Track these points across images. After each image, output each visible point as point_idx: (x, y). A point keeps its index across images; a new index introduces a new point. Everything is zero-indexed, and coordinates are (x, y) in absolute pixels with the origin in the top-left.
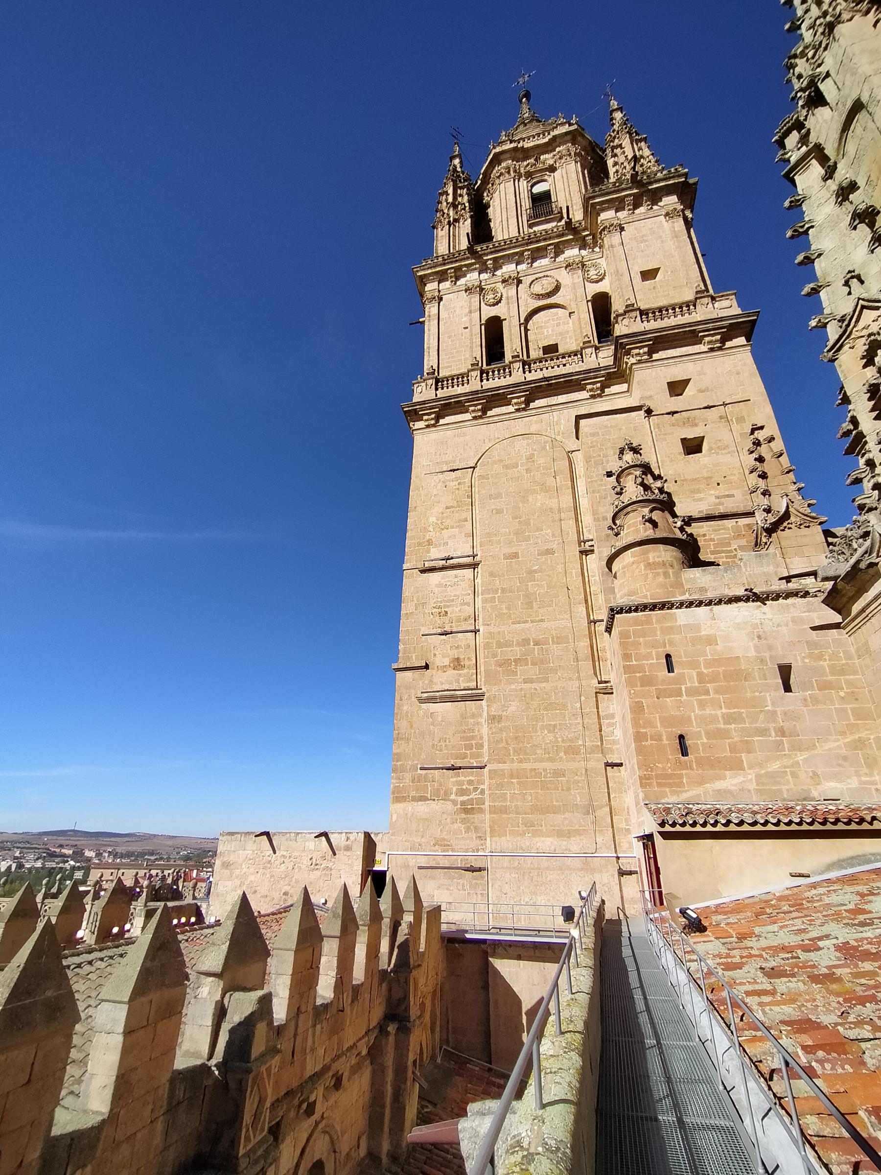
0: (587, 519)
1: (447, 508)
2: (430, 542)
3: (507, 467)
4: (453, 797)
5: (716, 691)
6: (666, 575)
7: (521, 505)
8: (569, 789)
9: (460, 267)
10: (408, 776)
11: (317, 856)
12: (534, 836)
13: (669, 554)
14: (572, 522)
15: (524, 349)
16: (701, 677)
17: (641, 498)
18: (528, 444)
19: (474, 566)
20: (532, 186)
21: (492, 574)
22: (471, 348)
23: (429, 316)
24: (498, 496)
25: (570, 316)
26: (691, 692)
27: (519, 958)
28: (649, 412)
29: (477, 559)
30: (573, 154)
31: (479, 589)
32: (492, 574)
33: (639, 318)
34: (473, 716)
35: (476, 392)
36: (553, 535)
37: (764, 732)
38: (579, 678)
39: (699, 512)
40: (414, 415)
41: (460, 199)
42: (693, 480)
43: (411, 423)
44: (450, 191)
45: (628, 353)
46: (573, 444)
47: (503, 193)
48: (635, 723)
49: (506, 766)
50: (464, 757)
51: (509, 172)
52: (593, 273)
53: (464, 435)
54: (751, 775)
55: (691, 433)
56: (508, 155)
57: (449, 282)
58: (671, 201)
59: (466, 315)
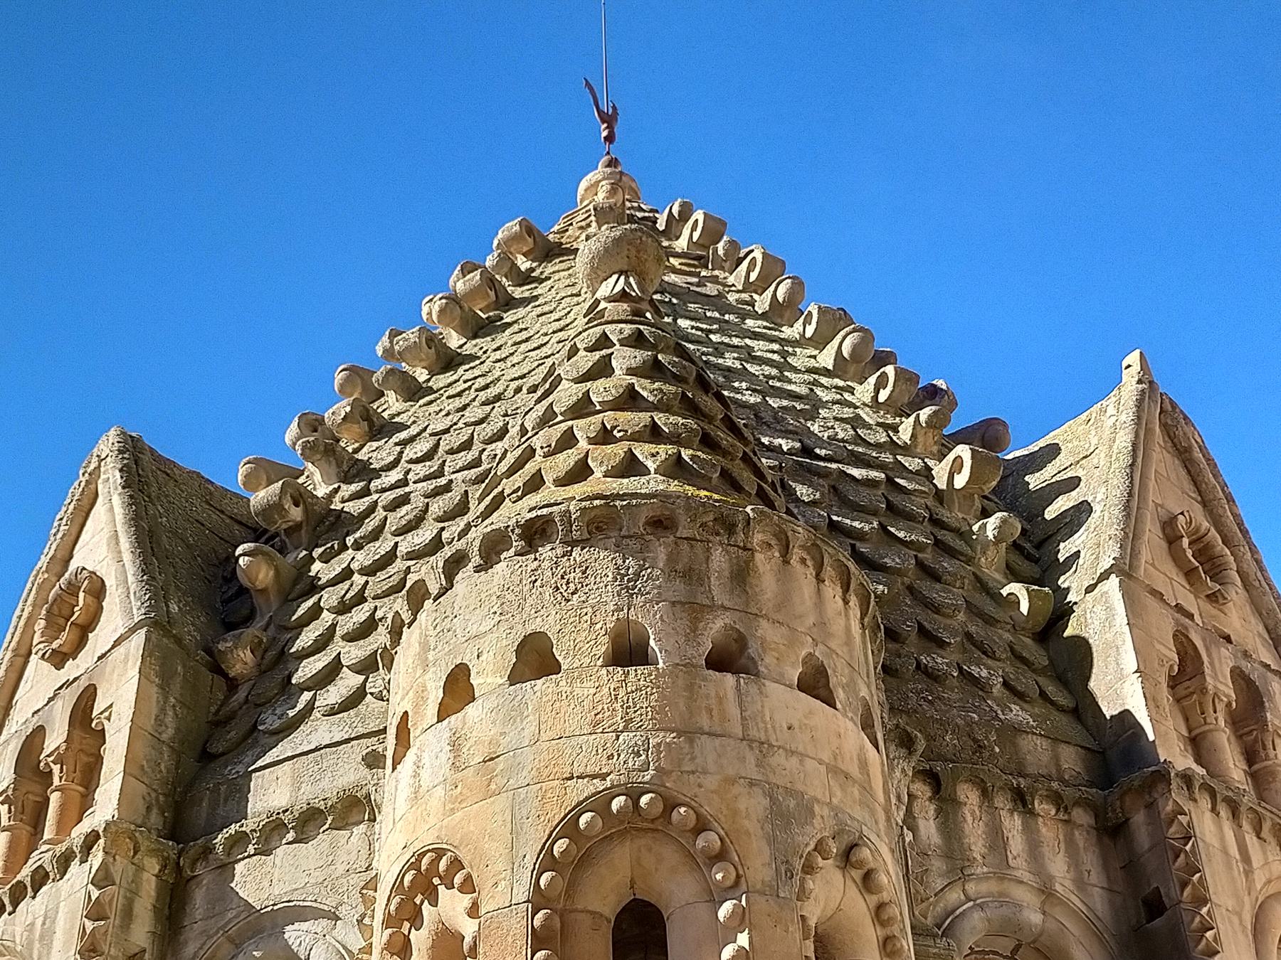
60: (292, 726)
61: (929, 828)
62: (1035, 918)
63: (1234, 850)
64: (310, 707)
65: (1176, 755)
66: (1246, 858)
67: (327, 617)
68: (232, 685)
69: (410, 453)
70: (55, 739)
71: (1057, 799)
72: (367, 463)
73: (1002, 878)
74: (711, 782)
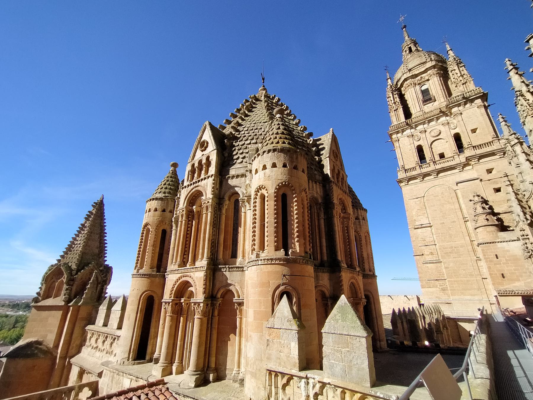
0: (465, 211)
1: (418, 210)
2: (415, 220)
3: (435, 196)
4: (438, 287)
5: (511, 263)
6: (493, 234)
7: (442, 208)
8: (472, 285)
9: (403, 129)
10: (424, 282)
11: (405, 301)
12: (464, 296)
13: (493, 228)
14: (460, 212)
15: (433, 156)
16: (506, 260)
17: (482, 213)
18: (441, 189)
19: (431, 227)
20: (421, 88)
21: (437, 229)
22: (414, 157)
23: (396, 147)
24: (434, 205)
25: (457, 185)
26: (503, 263)
27: (465, 322)
28: (481, 180)
29: (431, 224)
30: (435, 74)
31: (434, 233)
32: (437, 229)
33: (473, 149)
34: (440, 267)
35: (420, 174)
36: (455, 217)
37: (526, 273)
38: (470, 257)
39: (502, 211)
40: (400, 181)
41: (396, 99)
42: (499, 201)
43: (399, 184)
44: (391, 95)
45: (471, 161)
46: (455, 187)
47: (410, 93)
48: (489, 271)
49: (453, 279)
50: (440, 277)
51: (411, 85)
52: (452, 126)
53: (418, 186)
54: (523, 282)
55: (497, 186)
56: (410, 78)
57: (400, 134)
58: (479, 101)
59: (409, 145)
60: (234, 164)
62: (316, 195)
64: (236, 162)
65: (332, 179)
68: (225, 157)
69: (245, 129)
71: (319, 183)
72: (239, 130)
73: (313, 191)
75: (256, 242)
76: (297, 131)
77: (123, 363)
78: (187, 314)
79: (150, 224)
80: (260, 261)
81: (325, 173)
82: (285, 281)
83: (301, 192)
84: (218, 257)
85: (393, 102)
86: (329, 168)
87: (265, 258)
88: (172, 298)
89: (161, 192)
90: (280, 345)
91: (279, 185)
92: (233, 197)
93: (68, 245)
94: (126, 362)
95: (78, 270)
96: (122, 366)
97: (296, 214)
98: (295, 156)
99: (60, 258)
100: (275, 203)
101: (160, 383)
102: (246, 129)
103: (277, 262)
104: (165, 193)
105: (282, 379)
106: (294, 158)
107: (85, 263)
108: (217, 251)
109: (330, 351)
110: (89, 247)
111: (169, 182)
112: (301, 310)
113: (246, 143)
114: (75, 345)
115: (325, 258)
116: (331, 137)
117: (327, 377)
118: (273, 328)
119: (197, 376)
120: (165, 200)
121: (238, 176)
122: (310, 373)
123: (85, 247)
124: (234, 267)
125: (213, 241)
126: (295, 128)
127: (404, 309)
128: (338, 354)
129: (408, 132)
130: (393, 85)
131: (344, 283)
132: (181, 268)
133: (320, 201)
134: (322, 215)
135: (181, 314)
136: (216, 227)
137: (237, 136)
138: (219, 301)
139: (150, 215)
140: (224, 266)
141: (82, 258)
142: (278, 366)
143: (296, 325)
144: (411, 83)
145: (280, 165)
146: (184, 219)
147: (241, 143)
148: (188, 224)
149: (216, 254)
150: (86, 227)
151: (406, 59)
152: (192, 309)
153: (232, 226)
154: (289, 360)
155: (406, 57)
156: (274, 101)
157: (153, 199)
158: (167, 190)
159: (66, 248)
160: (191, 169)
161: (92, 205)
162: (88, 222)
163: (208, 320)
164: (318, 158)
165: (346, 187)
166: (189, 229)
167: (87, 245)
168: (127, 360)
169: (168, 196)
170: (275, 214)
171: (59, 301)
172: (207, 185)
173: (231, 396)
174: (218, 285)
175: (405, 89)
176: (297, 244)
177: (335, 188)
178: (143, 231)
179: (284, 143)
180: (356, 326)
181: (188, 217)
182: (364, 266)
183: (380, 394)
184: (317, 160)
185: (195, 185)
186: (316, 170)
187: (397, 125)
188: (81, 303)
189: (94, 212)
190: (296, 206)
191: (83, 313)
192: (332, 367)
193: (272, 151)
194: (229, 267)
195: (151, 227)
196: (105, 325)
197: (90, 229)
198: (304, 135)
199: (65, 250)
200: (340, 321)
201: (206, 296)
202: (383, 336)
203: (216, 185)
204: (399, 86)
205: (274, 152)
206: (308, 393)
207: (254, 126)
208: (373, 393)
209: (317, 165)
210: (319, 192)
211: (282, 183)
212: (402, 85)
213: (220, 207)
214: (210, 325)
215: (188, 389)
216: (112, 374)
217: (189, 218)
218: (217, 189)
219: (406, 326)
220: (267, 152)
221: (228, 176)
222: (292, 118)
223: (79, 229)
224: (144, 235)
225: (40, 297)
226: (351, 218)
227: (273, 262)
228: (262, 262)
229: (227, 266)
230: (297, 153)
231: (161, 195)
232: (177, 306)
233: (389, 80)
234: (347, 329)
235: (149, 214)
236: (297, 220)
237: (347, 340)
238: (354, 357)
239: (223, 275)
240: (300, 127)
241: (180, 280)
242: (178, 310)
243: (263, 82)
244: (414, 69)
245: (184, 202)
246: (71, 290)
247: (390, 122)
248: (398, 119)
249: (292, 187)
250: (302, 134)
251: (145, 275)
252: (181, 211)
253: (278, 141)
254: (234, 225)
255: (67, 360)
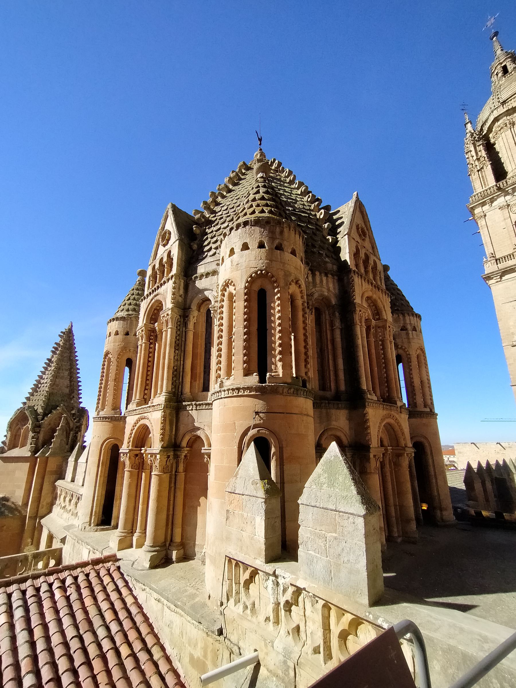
9: (493, 198)
23: (481, 226)
40: (488, 278)
41: (479, 154)
44: (472, 149)
51: (506, 126)
57: (488, 205)
61: (310, 279)
62: (326, 294)
63: (360, 284)
66: (362, 285)
67: (209, 239)
68: (194, 251)
70: (165, 260)
74: (275, 269)
75: (221, 366)
76: (302, 203)
77: (85, 529)
78: (151, 469)
79: (110, 353)
80: (223, 393)
81: (342, 260)
82: (258, 422)
83: (288, 284)
84: (183, 391)
85: (475, 158)
86: (347, 251)
87: (229, 387)
88: (130, 448)
89: (123, 310)
90: (242, 519)
91: (252, 275)
92: (203, 305)
93: (34, 385)
94: (88, 528)
95: (45, 415)
96: (83, 532)
97: (279, 318)
98: (278, 230)
99: (25, 401)
100: (246, 303)
101: (109, 559)
102: (225, 208)
103: (246, 393)
104: (128, 310)
105: (244, 571)
106: (277, 233)
107: (53, 405)
108: (182, 382)
109: (309, 535)
110: (57, 386)
111: (134, 296)
112: (283, 465)
113: (222, 227)
114: (45, 503)
115: (343, 387)
116: (353, 205)
117: (303, 578)
118: (234, 493)
119: (154, 553)
120: (128, 320)
121: (207, 275)
122: (280, 568)
123: (52, 386)
124: (202, 404)
125: (175, 368)
126: (298, 199)
127: (488, 463)
128: (320, 541)
129: (501, 201)
130: (475, 131)
131: (371, 424)
132: (140, 407)
133: (334, 301)
134: (337, 323)
135: (143, 469)
136: (180, 349)
137: (212, 219)
138: (185, 452)
139: (110, 340)
140: (190, 403)
141: (49, 399)
142: (239, 552)
143: (263, 490)
144: (506, 123)
145: (253, 245)
146: (143, 342)
147: (215, 229)
148: (150, 348)
149: (180, 386)
150: (52, 363)
151: (498, 86)
152: (149, 462)
153: (204, 346)
154: (253, 545)
155: (497, 83)
156: (273, 168)
157: (113, 320)
158: (131, 307)
159: (32, 389)
160: (151, 273)
161: (59, 335)
162: (55, 356)
163: (170, 478)
164: (332, 238)
165: (381, 281)
166: (150, 355)
167: (54, 384)
168: (88, 525)
169: (132, 315)
170: (245, 320)
171: (25, 451)
172: (167, 292)
173: (192, 585)
174: (182, 429)
175: (494, 134)
176: (280, 364)
177: (357, 280)
178: (104, 361)
179: (263, 211)
180: (349, 495)
181: (149, 339)
182: (415, 399)
183: (383, 621)
184: (330, 241)
185: (155, 293)
186: (327, 256)
187: (482, 193)
188: (48, 454)
189: (61, 343)
190: (278, 306)
191: (52, 465)
192: (310, 562)
193: (242, 226)
194: (195, 404)
195: (111, 356)
196: (73, 481)
197: (57, 364)
198: (312, 208)
199: (31, 391)
200: (326, 485)
201: (165, 445)
202: (447, 502)
203: (177, 290)
204: (485, 132)
205: (245, 226)
206: (277, 599)
207: (236, 203)
208: (371, 618)
209: (330, 248)
210: (331, 288)
211: (256, 273)
212: (490, 130)
213: (185, 321)
214: (173, 485)
215: (141, 570)
216: (73, 541)
217: (150, 339)
218: (180, 296)
219: (490, 487)
220: (235, 228)
221: (195, 275)
222: (296, 186)
223: (45, 366)
224: (105, 367)
225: (7, 446)
226: (389, 327)
227: (240, 394)
228: (226, 394)
229: (194, 403)
230: (282, 225)
231: (124, 314)
232: (137, 458)
233: (469, 126)
234: (335, 500)
235: (109, 339)
236: (280, 328)
237: (335, 519)
238: (345, 549)
239: (188, 416)
240: (307, 196)
241: (138, 423)
242: (139, 463)
243: (260, 144)
244: (511, 100)
245: (144, 318)
246: (38, 439)
247: (470, 189)
248: (484, 183)
249: (273, 276)
250: (309, 206)
251: (106, 418)
252: (140, 331)
253: (254, 210)
254: (206, 344)
255: (38, 520)
